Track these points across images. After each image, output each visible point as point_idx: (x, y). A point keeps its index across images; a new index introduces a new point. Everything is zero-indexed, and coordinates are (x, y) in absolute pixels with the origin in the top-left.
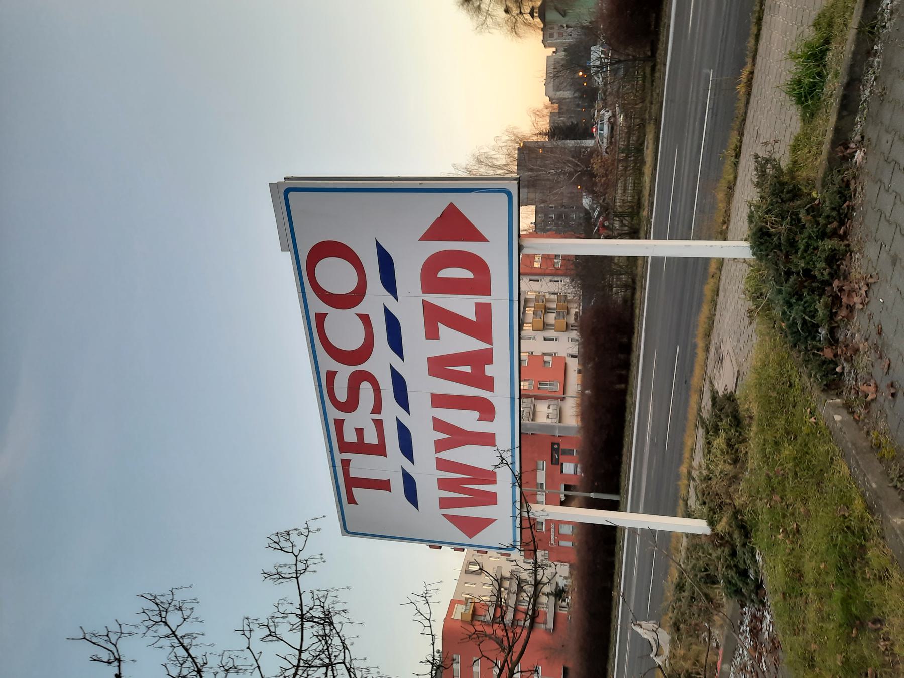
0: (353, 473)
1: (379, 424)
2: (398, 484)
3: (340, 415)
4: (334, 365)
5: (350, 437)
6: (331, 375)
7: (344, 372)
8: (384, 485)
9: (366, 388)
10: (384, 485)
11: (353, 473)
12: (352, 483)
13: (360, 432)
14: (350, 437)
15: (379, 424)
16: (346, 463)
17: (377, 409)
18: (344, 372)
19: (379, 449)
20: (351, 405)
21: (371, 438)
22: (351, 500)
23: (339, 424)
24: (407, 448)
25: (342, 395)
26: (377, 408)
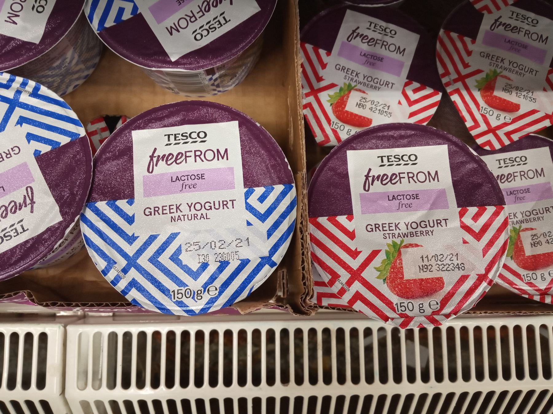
0: (501, 161)
1: (508, 163)
4: (514, 158)
5: (506, 160)
7: (514, 159)
8: (500, 164)
9: (512, 162)
10: (500, 164)
14: (506, 160)
15: (508, 163)
16: (502, 160)
18: (514, 159)
21: (506, 162)
23: (507, 159)
24: (505, 167)
25: (511, 159)
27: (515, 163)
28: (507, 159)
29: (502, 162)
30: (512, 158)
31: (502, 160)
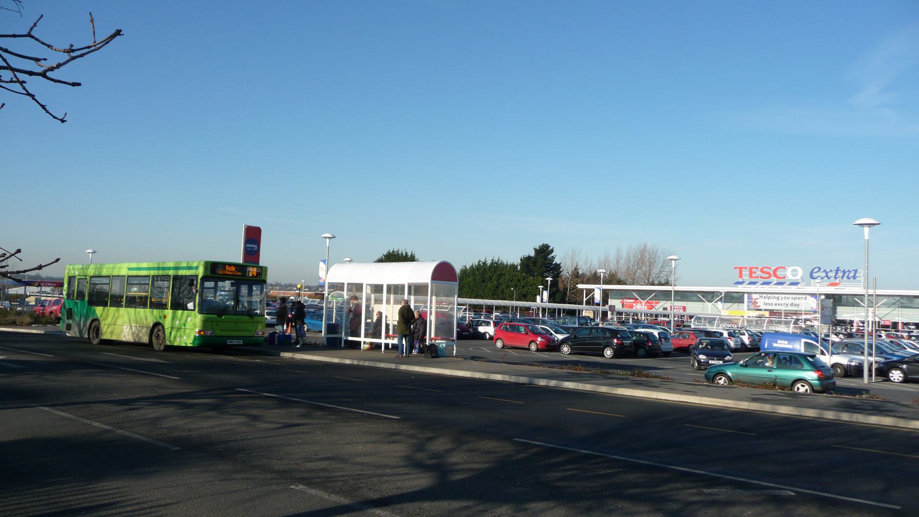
0: (743, 269)
1: (758, 277)
2: (740, 280)
3: (760, 268)
6: (770, 268)
8: (741, 276)
9: (767, 276)
10: (741, 276)
11: (743, 269)
12: (741, 269)
13: (755, 273)
14: (754, 270)
15: (758, 277)
16: (746, 268)
17: (761, 277)
19: (751, 276)
20: (762, 271)
22: (735, 268)
23: (757, 268)
25: (765, 270)
26: (761, 277)
27: (774, 280)
28: (757, 268)
29: (746, 273)
30: (770, 268)
31: (746, 268)
